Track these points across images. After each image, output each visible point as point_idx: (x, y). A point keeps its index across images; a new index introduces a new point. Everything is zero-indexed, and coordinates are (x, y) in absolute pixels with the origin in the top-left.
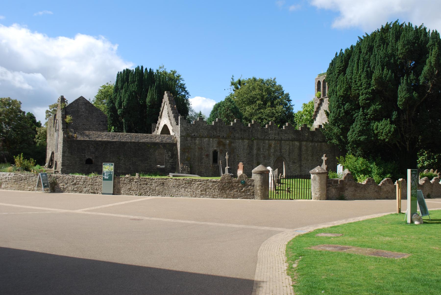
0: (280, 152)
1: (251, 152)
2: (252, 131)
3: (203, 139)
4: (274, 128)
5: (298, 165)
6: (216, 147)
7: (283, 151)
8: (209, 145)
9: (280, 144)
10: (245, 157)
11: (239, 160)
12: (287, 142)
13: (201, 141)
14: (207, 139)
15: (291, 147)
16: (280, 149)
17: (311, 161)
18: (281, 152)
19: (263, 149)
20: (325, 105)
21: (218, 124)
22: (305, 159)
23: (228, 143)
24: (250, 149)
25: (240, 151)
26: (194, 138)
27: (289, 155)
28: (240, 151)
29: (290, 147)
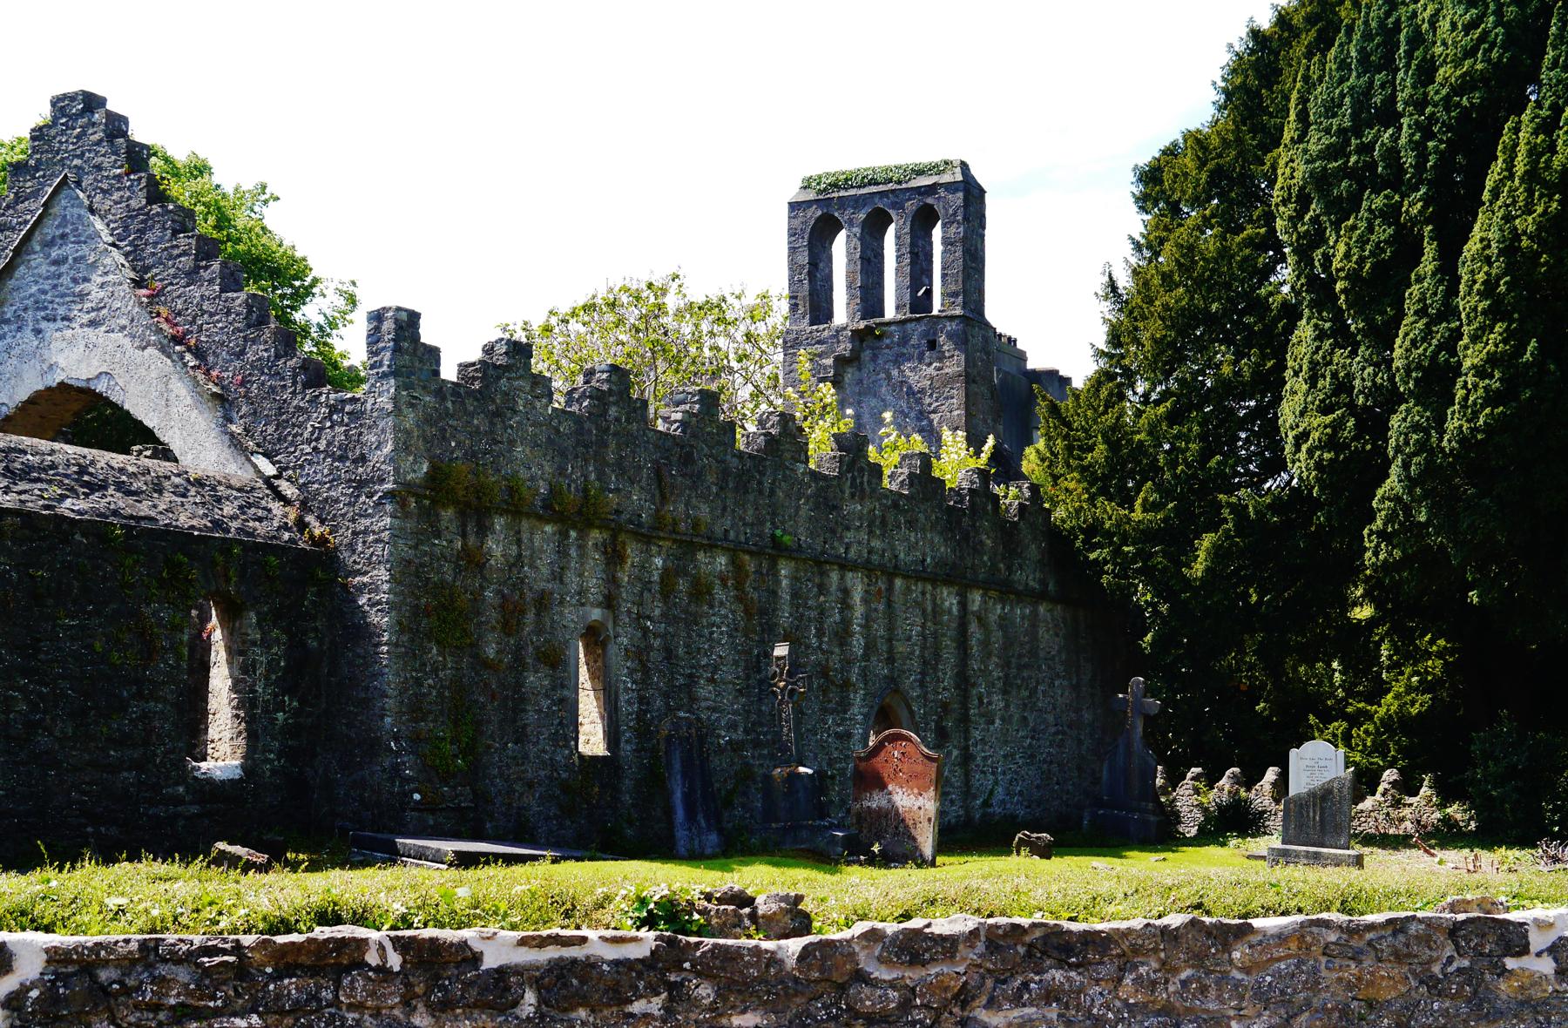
2: (772, 493)
3: (525, 524)
4: (865, 479)
5: (955, 753)
6: (599, 605)
7: (901, 648)
8: (562, 582)
9: (889, 604)
11: (714, 710)
12: (917, 588)
13: (519, 542)
14: (548, 529)
17: (1003, 719)
18: (891, 660)
20: (895, 373)
22: (982, 710)
26: (476, 512)
29: (923, 626)
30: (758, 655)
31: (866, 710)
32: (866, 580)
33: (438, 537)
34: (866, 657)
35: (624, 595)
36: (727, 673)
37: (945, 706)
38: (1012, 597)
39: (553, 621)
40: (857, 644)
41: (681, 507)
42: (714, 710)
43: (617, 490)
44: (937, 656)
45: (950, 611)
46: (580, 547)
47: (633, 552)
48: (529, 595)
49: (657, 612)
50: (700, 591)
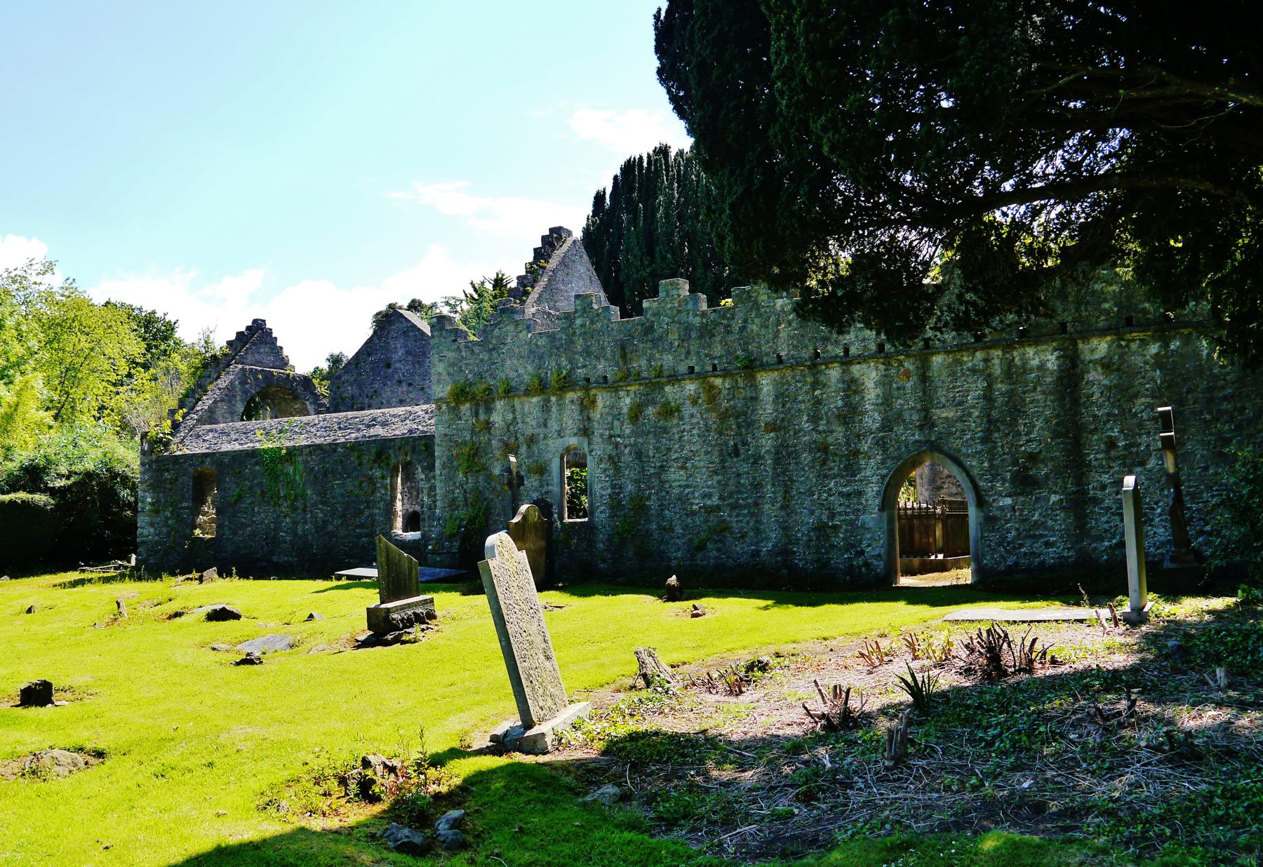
0: (921, 428)
1: (745, 443)
3: (517, 402)
5: (1054, 498)
6: (575, 435)
8: (545, 425)
10: (716, 473)
11: (687, 486)
13: (514, 412)
14: (535, 400)
15: (1001, 387)
16: (926, 411)
18: (927, 423)
19: (814, 419)
21: (578, 322)
23: (625, 410)
24: (739, 426)
25: (690, 442)
26: (485, 401)
27: (984, 440)
28: (690, 442)
29: (990, 387)
30: (736, 445)
31: (885, 472)
32: (882, 367)
33: (460, 419)
34: (887, 425)
35: (596, 425)
36: (701, 461)
37: (1033, 458)
38: (1186, 332)
39: (539, 449)
40: (872, 419)
41: (644, 363)
42: (687, 486)
43: (584, 366)
44: (1015, 409)
45: (1042, 367)
46: (559, 405)
47: (603, 400)
48: (521, 439)
49: (628, 431)
50: (669, 411)
